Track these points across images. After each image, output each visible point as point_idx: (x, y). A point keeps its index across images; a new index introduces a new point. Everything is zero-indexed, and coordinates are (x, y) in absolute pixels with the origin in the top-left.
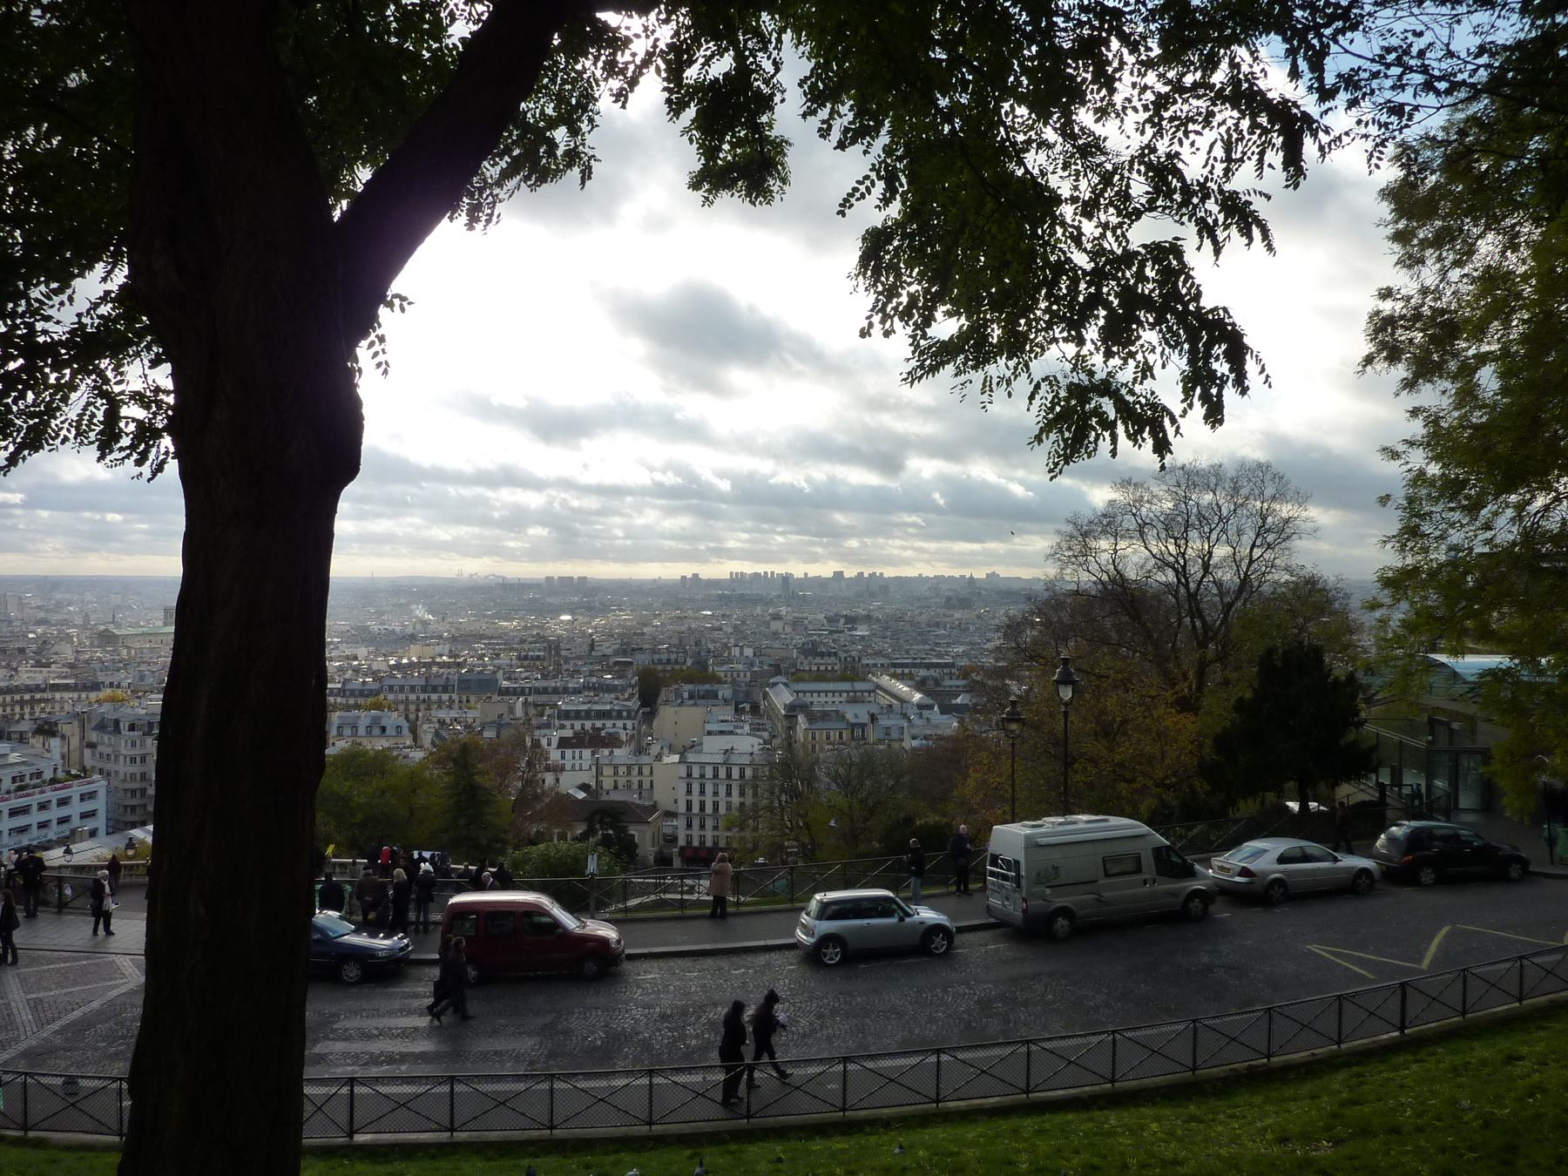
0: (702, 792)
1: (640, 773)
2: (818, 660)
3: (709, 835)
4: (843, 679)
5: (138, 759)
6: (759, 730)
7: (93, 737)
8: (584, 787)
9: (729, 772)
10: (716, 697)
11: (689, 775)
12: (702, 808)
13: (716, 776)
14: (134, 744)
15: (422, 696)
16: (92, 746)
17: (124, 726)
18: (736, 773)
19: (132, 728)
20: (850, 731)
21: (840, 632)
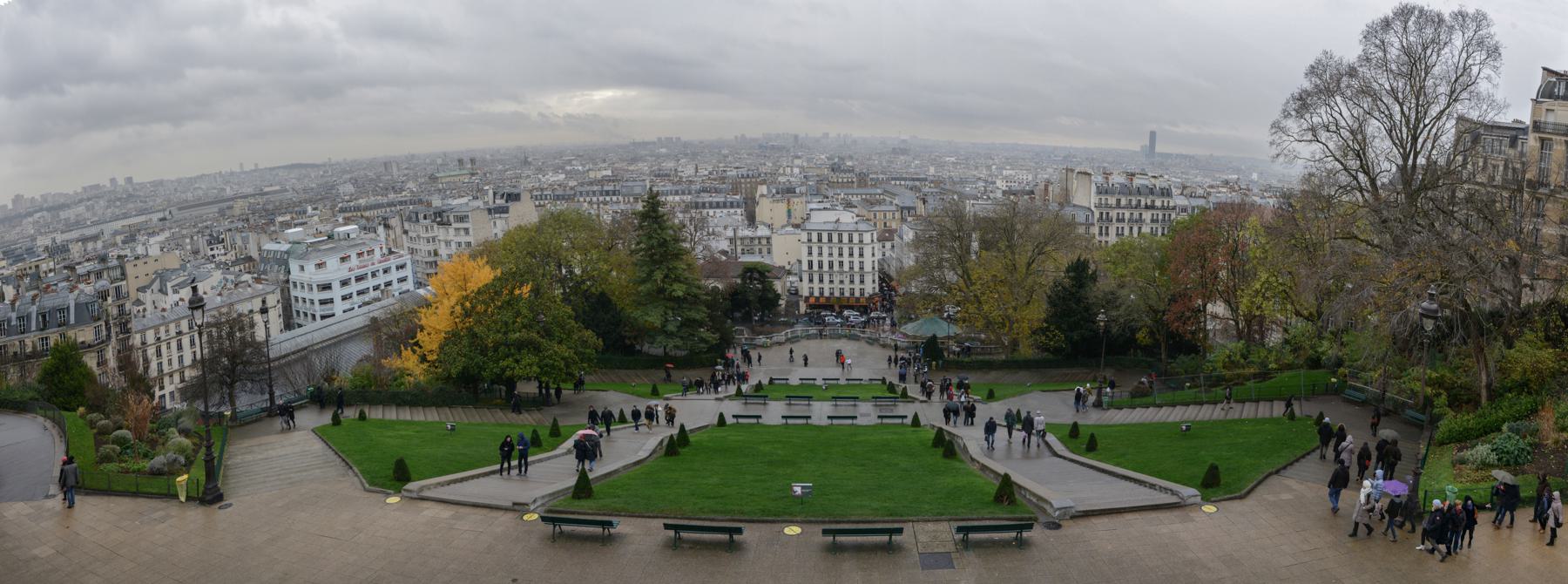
0: (820, 254)
1: (760, 243)
2: (842, 175)
3: (826, 286)
4: (859, 186)
5: (431, 240)
6: (851, 207)
7: (407, 226)
8: (724, 253)
9: (840, 236)
10: (795, 192)
11: (810, 241)
12: (821, 265)
13: (830, 240)
14: (427, 230)
15: (601, 199)
16: (406, 232)
17: (421, 216)
18: (845, 238)
19: (425, 218)
20: (900, 212)
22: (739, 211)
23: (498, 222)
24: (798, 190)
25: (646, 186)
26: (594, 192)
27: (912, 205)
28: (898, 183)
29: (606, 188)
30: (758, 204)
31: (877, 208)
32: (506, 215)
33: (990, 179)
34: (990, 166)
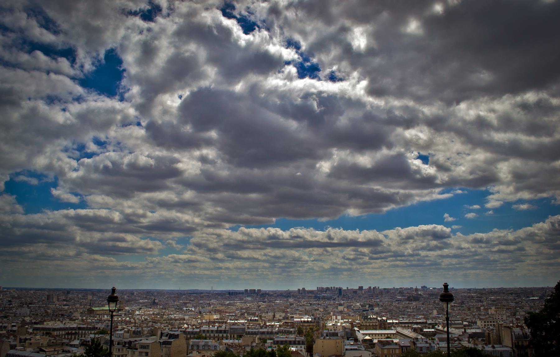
4: (381, 328)
6: (369, 348)
15: (216, 335)
21: (368, 310)
22: (303, 346)
23: (164, 349)
24: (339, 335)
25: (245, 328)
26: (212, 331)
27: (409, 345)
28: (407, 325)
29: (220, 329)
30: (315, 342)
31: (387, 347)
32: (170, 346)
33: (474, 320)
34: (480, 308)
